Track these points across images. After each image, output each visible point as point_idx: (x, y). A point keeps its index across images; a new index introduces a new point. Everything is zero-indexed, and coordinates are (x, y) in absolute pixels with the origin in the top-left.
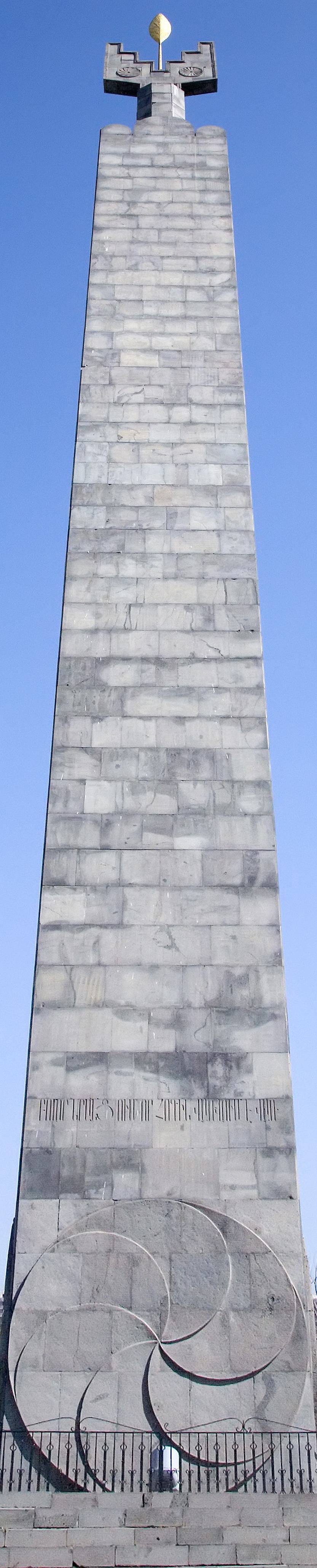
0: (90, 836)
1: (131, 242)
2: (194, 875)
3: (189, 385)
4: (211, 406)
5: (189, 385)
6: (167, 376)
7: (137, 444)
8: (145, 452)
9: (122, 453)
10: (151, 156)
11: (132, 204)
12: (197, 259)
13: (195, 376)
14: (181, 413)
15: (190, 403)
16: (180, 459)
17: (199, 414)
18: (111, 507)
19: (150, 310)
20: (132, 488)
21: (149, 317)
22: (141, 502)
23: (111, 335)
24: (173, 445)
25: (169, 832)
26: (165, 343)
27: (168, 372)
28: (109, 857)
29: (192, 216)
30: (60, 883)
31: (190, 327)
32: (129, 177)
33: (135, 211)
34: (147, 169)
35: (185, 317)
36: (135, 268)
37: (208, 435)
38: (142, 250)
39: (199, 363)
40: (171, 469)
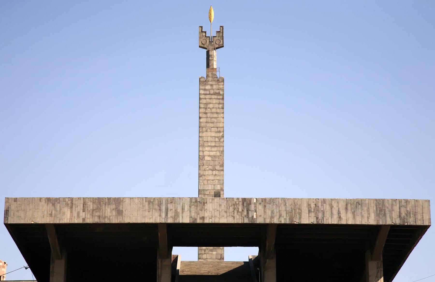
0: (203, 252)
1: (206, 122)
2: (214, 257)
3: (215, 165)
4: (219, 170)
5: (215, 165)
6: (212, 163)
7: (208, 180)
8: (209, 182)
9: (205, 182)
10: (209, 90)
11: (206, 108)
12: (217, 128)
13: (217, 163)
14: (214, 172)
15: (216, 170)
16: (214, 184)
17: (217, 173)
18: (204, 194)
19: (209, 144)
20: (207, 190)
21: (209, 146)
22: (208, 193)
23: (203, 152)
24: (213, 180)
25: (212, 251)
26: (212, 154)
27: (212, 162)
28: (205, 255)
29: (217, 113)
30: (200, 259)
31: (215, 149)
32: (205, 99)
33: (207, 112)
34: (209, 95)
35: (215, 146)
36: (206, 131)
37: (218, 178)
38: (208, 125)
39: (217, 159)
40: (213, 186)
